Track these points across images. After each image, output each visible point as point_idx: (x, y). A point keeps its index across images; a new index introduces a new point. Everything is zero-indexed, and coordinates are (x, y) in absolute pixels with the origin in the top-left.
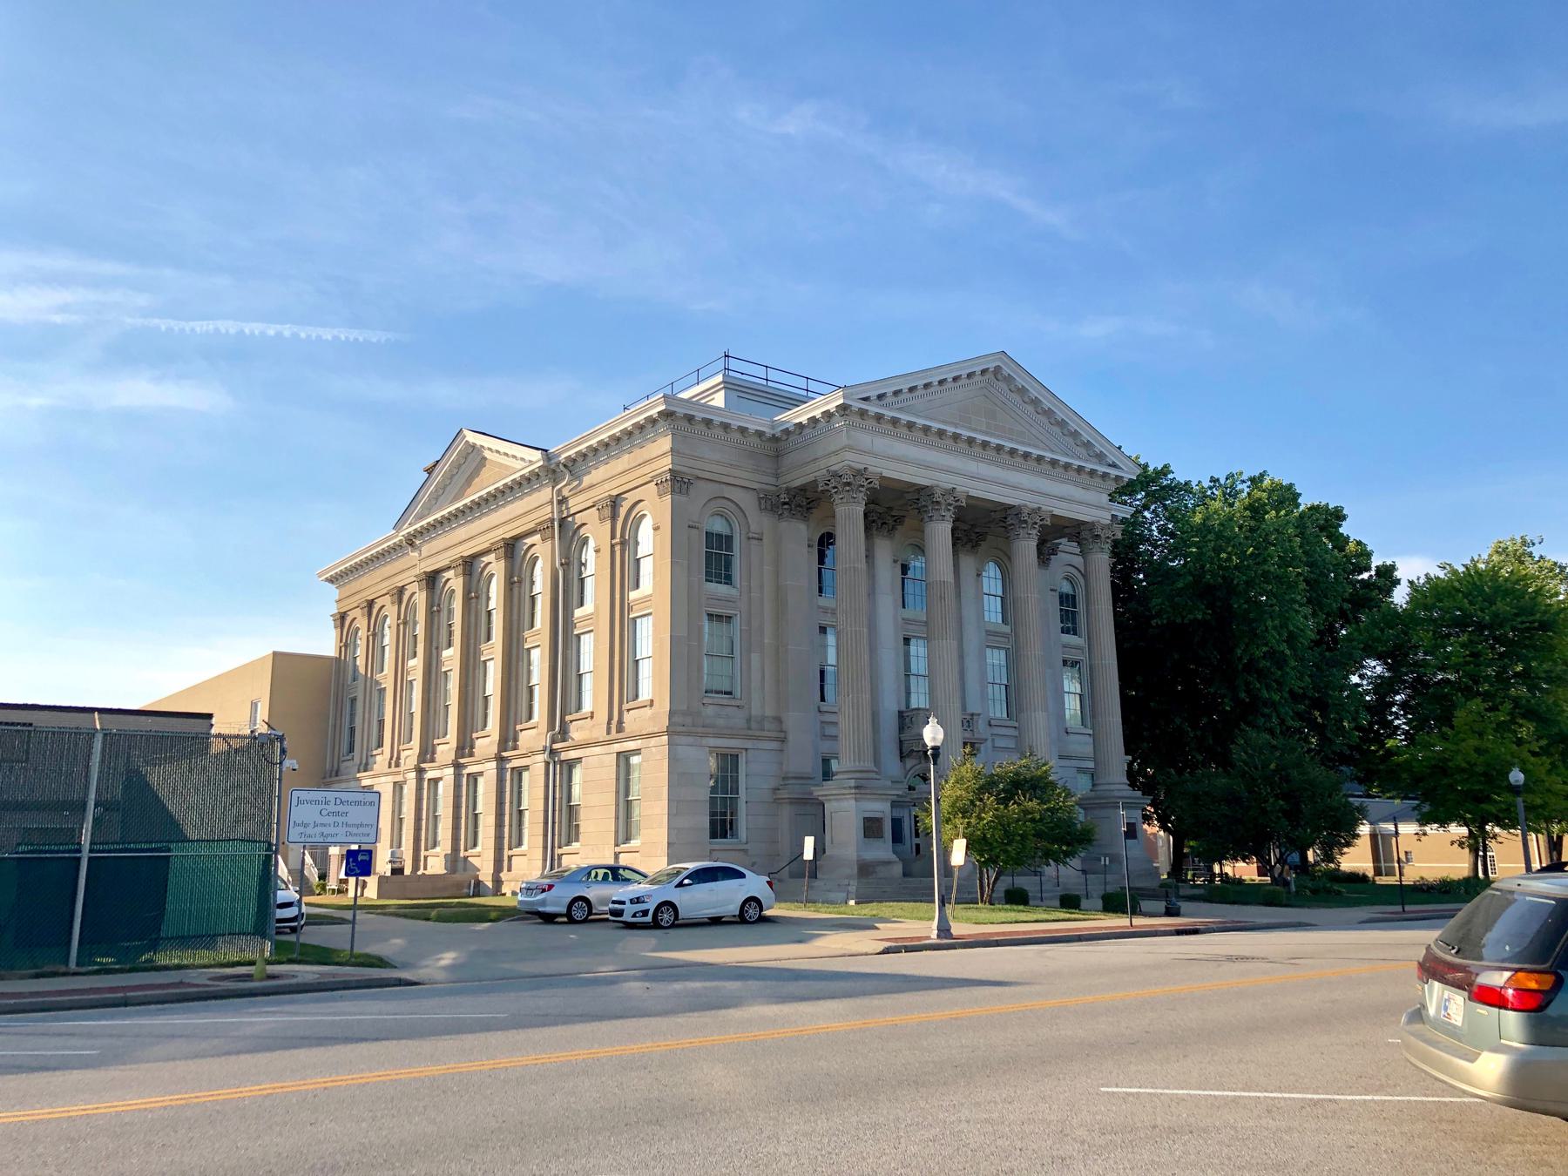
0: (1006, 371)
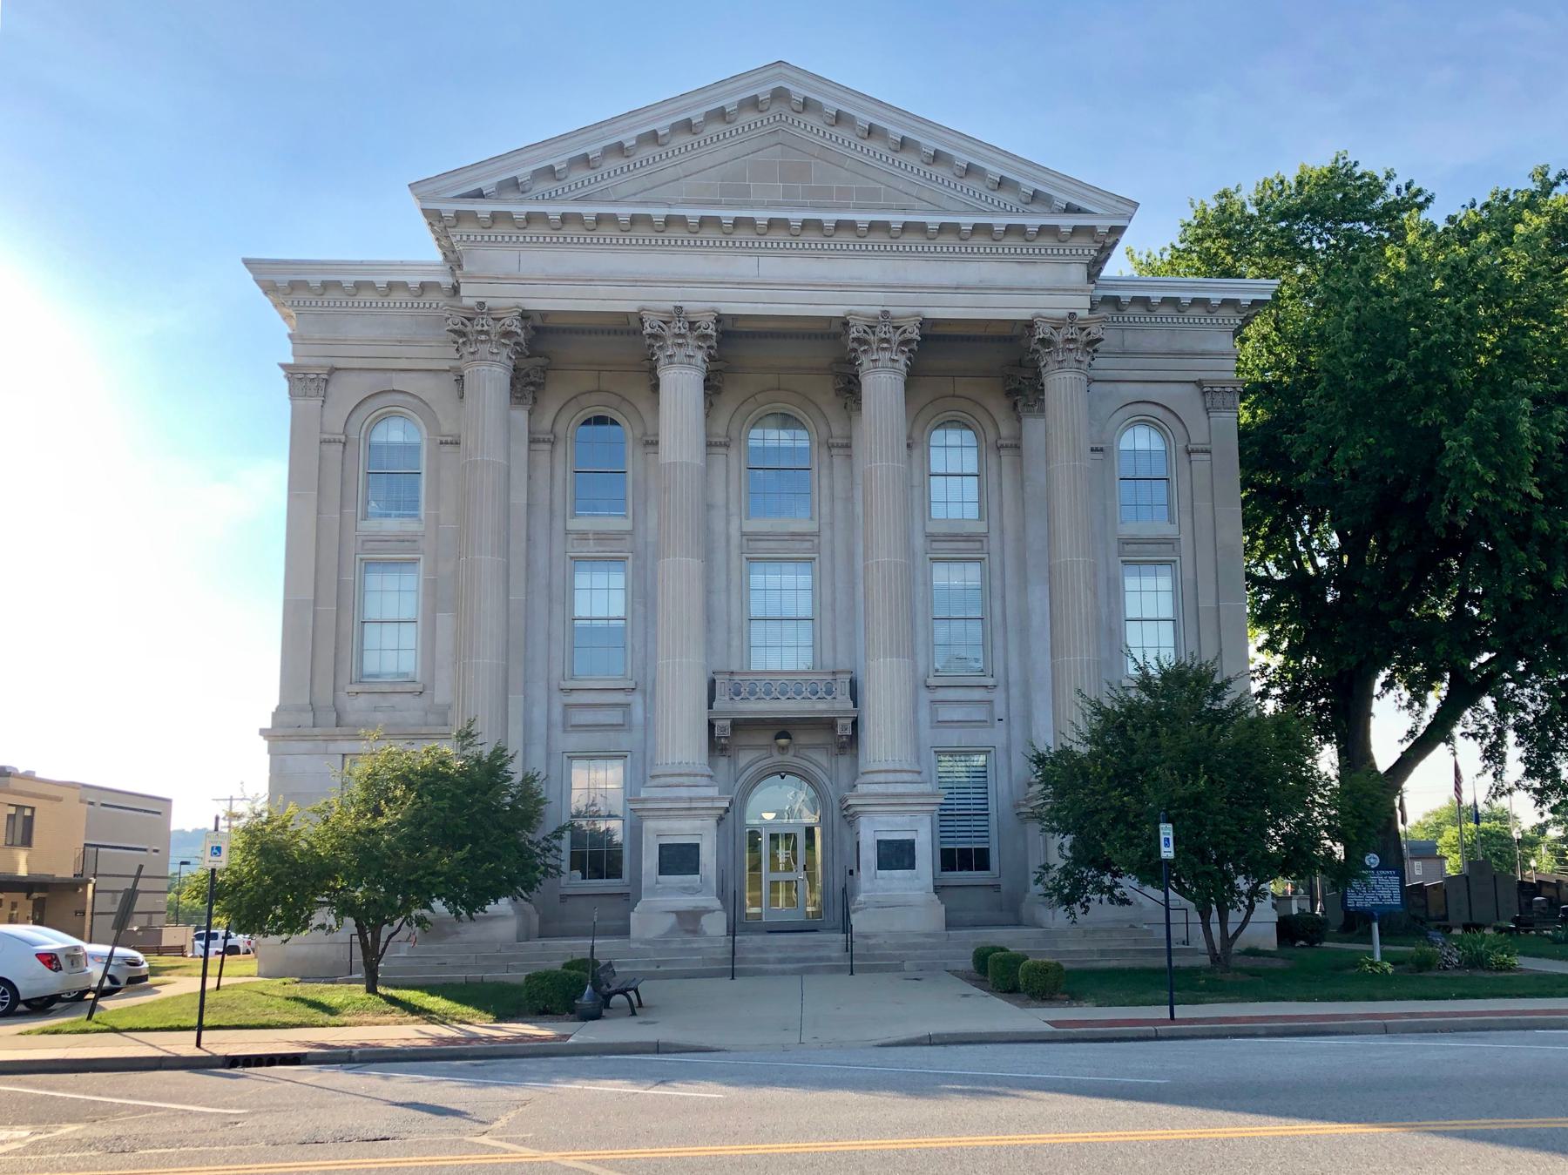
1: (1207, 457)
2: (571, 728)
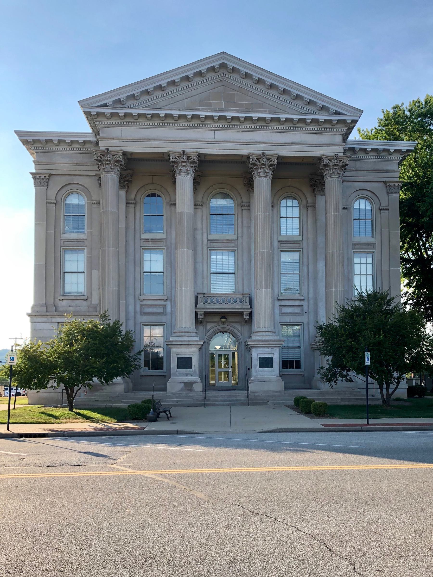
0: (230, 65)
1: (387, 211)
2: (143, 313)
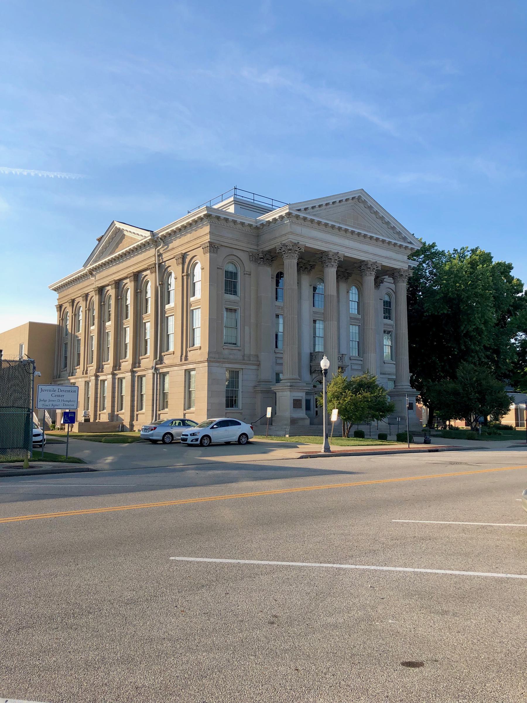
0: (363, 198)
